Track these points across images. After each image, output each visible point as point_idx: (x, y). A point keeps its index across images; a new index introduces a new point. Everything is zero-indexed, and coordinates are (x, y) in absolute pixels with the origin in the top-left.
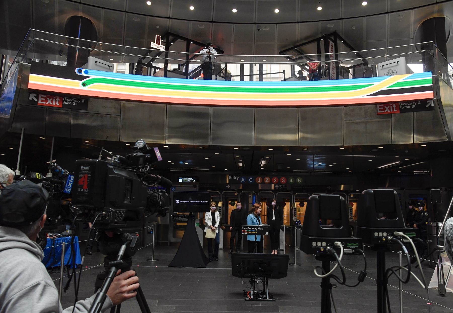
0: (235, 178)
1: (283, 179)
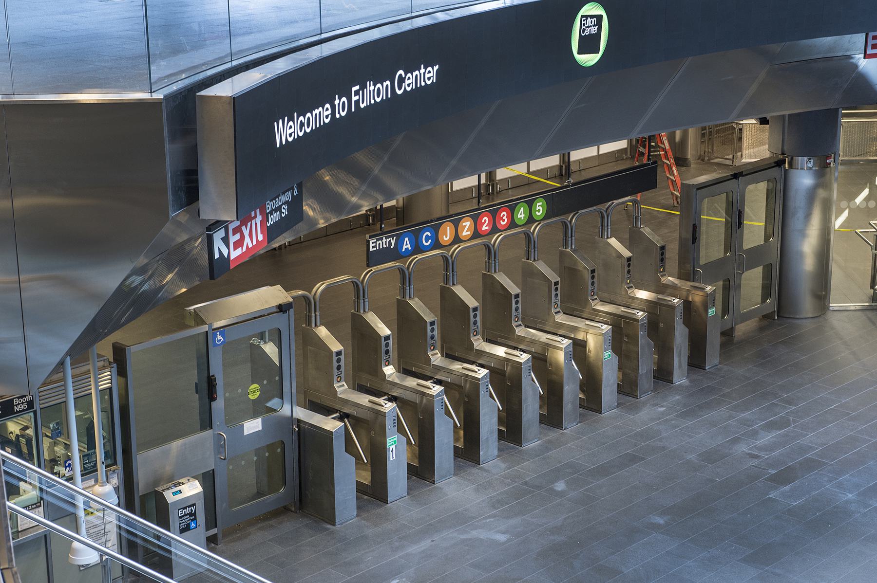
0: (386, 242)
1: (504, 215)
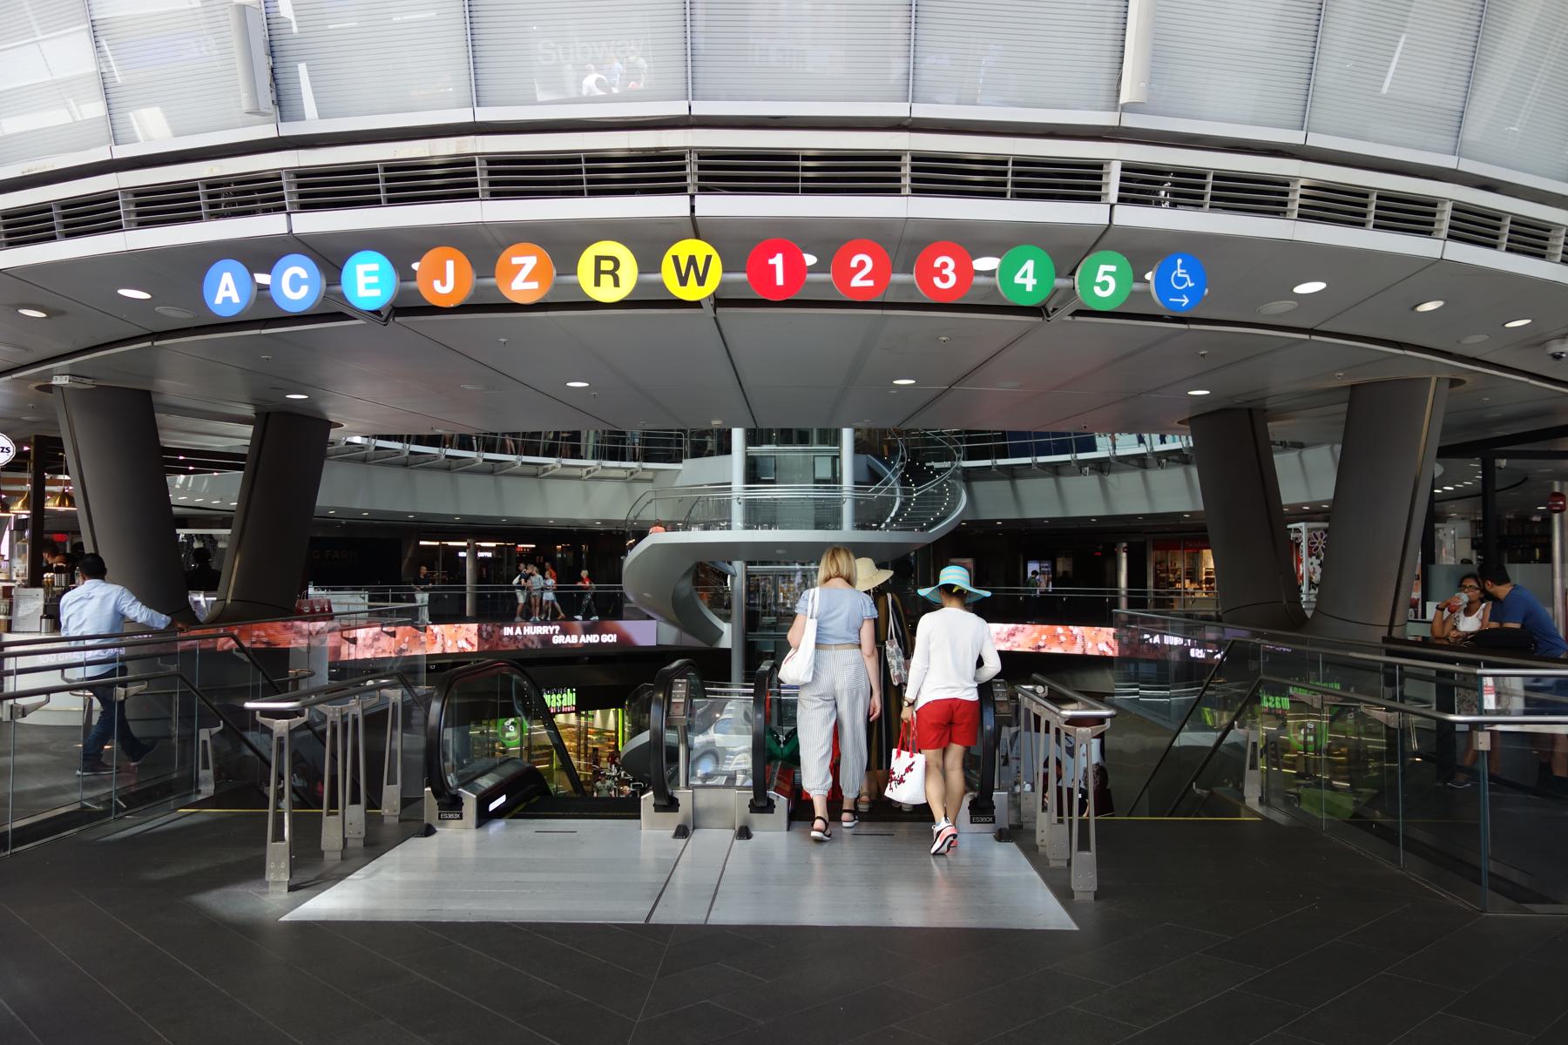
1: (945, 265)
